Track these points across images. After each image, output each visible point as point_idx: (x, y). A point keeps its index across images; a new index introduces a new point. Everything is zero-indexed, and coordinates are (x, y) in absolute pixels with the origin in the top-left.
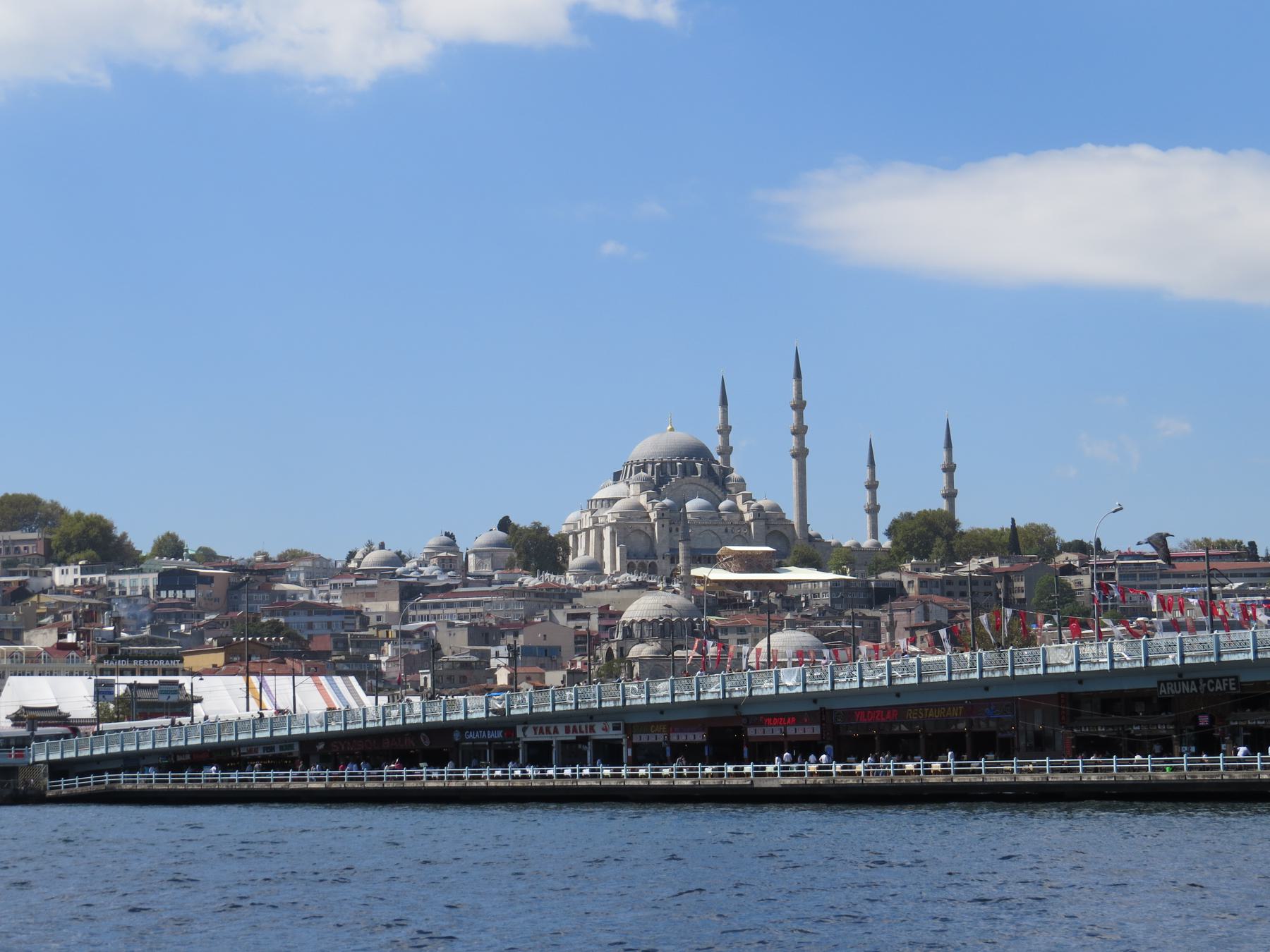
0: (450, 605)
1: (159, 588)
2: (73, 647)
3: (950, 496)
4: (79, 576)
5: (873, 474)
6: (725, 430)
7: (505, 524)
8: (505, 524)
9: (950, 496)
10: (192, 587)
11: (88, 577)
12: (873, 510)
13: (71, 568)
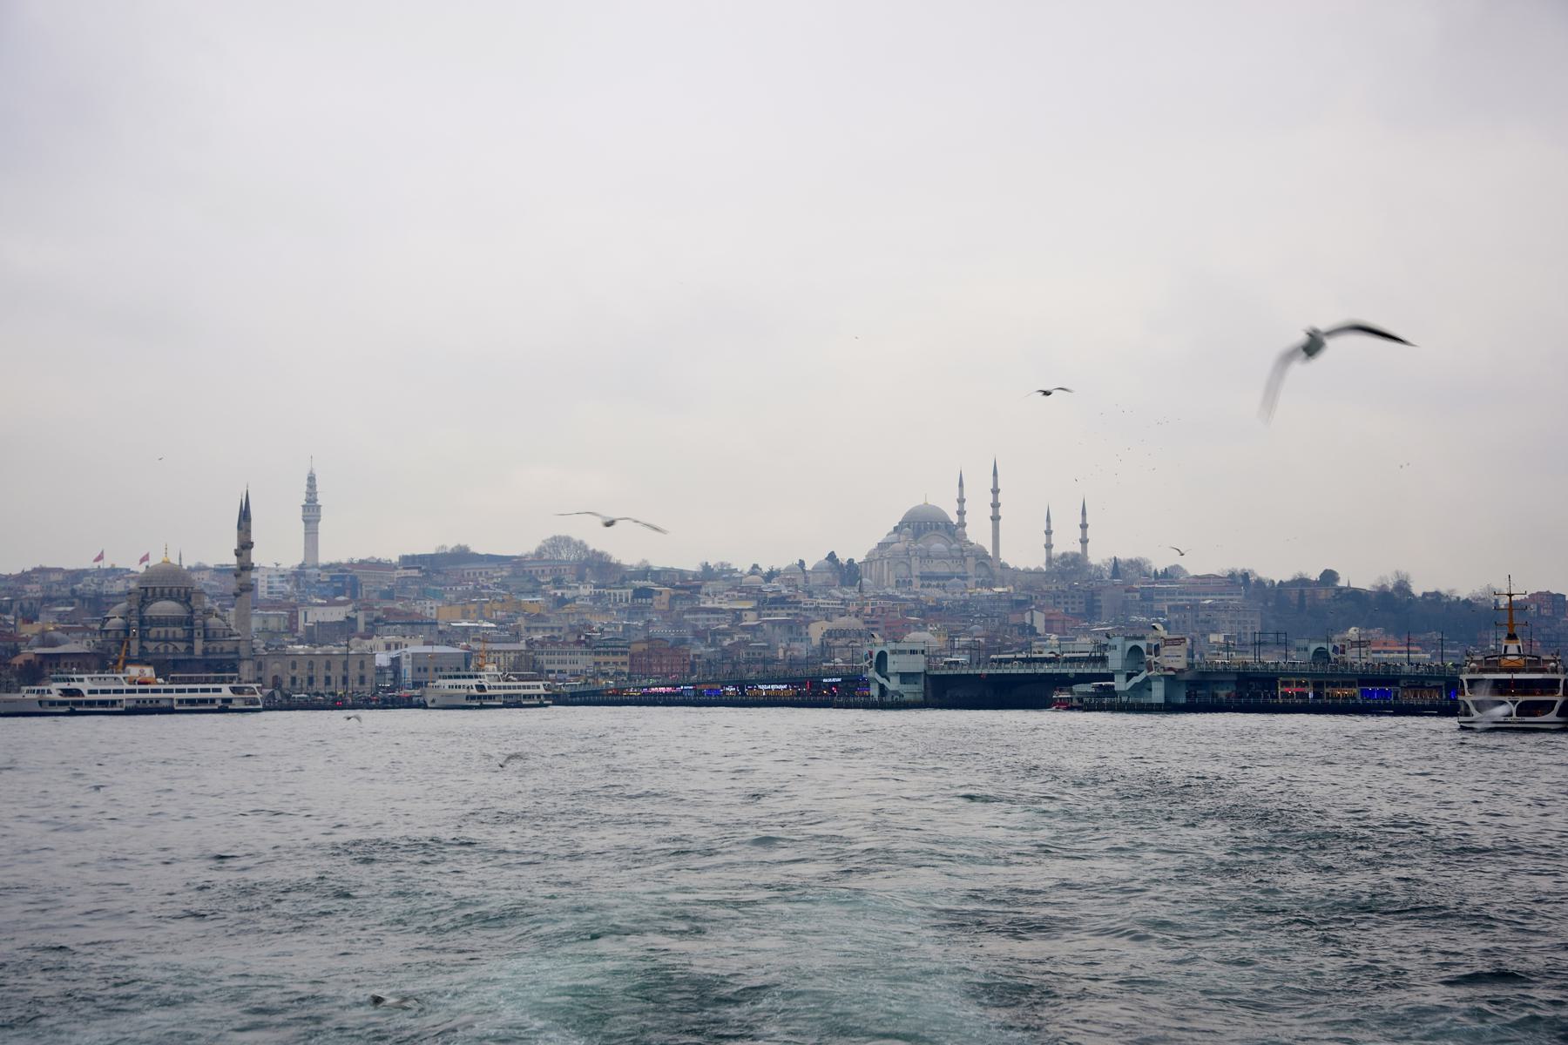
0: (783, 609)
1: (633, 598)
2: (584, 642)
3: (1084, 541)
4: (592, 590)
5: (1049, 526)
6: (961, 501)
7: (832, 557)
8: (832, 557)
9: (1084, 541)
10: (651, 597)
11: (597, 591)
12: (1049, 546)
13: (588, 586)
